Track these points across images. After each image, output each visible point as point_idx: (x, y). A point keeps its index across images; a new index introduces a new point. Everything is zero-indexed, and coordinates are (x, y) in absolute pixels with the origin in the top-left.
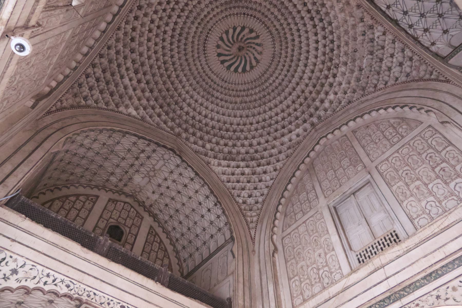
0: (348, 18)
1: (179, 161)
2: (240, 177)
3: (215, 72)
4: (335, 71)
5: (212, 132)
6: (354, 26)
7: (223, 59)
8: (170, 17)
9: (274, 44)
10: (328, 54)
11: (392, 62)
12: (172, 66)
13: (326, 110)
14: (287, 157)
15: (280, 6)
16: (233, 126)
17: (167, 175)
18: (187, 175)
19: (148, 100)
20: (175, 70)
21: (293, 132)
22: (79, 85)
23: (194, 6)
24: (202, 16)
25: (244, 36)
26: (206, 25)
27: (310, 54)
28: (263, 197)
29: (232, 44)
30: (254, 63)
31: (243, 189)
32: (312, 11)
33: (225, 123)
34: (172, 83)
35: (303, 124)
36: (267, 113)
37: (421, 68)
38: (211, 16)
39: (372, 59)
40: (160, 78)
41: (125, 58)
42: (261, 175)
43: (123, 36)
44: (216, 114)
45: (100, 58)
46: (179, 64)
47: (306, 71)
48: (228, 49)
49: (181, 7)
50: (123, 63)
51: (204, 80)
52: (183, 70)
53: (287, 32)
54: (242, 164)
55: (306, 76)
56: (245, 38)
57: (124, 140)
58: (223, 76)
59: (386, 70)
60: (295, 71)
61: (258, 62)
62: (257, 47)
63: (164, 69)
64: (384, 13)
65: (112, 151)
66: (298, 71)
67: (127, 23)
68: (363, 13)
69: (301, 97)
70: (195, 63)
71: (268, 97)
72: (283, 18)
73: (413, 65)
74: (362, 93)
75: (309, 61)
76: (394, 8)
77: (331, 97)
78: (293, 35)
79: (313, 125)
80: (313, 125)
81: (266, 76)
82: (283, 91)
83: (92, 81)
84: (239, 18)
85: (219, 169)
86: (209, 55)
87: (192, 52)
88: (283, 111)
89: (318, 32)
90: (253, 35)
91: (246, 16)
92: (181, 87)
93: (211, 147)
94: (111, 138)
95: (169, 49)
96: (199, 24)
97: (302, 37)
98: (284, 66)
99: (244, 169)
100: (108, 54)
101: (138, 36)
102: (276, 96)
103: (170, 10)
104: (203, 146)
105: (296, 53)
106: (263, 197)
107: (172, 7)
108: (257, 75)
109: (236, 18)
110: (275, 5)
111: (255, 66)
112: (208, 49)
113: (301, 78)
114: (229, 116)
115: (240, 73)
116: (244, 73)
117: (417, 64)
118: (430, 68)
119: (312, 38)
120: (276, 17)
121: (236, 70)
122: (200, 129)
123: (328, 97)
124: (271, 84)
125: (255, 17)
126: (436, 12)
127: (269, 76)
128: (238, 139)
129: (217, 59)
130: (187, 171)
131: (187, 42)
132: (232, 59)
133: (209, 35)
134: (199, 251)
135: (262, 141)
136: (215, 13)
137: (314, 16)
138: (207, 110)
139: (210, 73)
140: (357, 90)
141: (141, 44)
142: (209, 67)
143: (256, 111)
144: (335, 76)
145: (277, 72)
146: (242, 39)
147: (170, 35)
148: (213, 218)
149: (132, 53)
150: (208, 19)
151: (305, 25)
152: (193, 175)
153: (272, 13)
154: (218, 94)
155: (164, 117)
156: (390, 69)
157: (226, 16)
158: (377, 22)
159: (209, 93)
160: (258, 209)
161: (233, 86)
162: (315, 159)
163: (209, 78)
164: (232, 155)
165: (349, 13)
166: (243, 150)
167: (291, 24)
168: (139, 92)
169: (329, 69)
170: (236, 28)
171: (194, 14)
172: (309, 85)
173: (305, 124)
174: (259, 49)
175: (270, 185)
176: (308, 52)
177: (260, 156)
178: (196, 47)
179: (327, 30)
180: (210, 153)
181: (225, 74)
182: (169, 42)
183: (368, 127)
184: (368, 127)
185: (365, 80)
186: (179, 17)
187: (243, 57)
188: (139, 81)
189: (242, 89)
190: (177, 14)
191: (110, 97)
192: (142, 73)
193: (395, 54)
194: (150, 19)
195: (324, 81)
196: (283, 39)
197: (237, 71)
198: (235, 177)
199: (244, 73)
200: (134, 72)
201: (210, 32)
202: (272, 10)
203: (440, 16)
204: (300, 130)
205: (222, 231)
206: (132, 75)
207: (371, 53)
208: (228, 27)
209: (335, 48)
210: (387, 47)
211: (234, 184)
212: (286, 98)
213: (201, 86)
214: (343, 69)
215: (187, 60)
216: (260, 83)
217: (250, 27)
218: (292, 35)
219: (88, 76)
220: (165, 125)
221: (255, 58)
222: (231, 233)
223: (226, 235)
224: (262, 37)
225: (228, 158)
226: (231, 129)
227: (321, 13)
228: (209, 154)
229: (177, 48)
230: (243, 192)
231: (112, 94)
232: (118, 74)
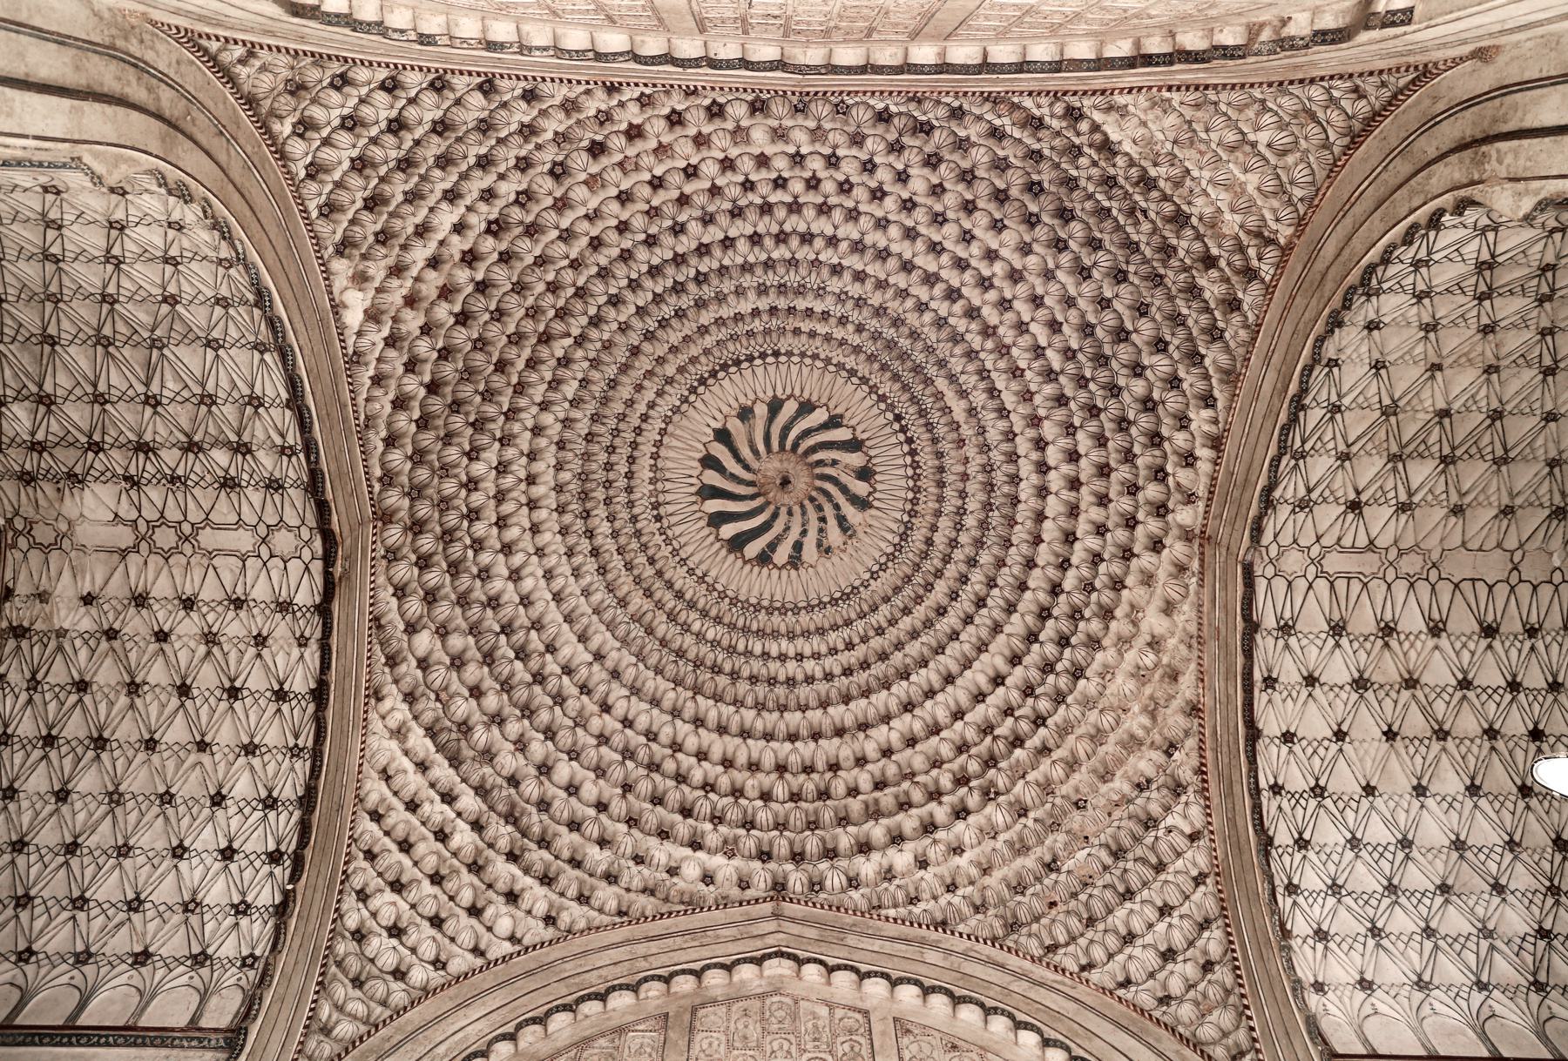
0: (1136, 708)
1: (306, 596)
2: (424, 839)
3: (660, 464)
4: (973, 801)
5: (476, 610)
6: (1133, 743)
8: (737, 213)
9: (883, 568)
10: (995, 738)
11: (1151, 926)
12: (584, 320)
13: (853, 882)
14: (620, 913)
16: (548, 657)
17: (210, 592)
18: (280, 660)
19: (426, 330)
20: (580, 341)
21: (700, 854)
22: (342, 76)
23: (816, 263)
24: (801, 304)
25: (835, 463)
26: (782, 331)
27: (950, 689)
28: (437, 977)
30: (782, 554)
31: (397, 886)
32: (1062, 598)
33: (537, 625)
34: (532, 363)
35: (751, 857)
36: (679, 723)
37: (1216, 1013)
38: (822, 329)
39: (1105, 868)
41: (524, 164)
42: (491, 894)
43: (592, 112)
44: (540, 573)
45: (480, 87)
46: (606, 336)
47: (895, 723)
48: (761, 448)
49: (787, 228)
50: (502, 169)
51: (611, 449)
52: (595, 363)
53: (947, 574)
54: (469, 801)
55: (880, 734)
56: (828, 471)
57: (240, 360)
58: (669, 497)
59: (1116, 932)
60: (866, 693)
61: (795, 561)
62: (832, 522)
63: (561, 303)
64: (1256, 792)
65: (156, 344)
66: (873, 698)
67: (644, 101)
68: (1187, 733)
69: (815, 776)
70: (646, 383)
71: (723, 681)
72: (976, 533)
73: (1201, 987)
74: (1000, 932)
75: (929, 704)
76: (1285, 805)
77: (901, 859)
79: (779, 887)
80: (779, 887)
81: (776, 619)
82: (783, 708)
83: (381, 109)
84: (875, 411)
85: (385, 748)
86: (699, 404)
87: (674, 350)
88: (728, 763)
89: (1027, 660)
90: (860, 488)
91: (896, 426)
92: (538, 399)
93: (431, 652)
94: (219, 311)
95: (634, 276)
97: (971, 629)
98: (850, 646)
99: (460, 824)
100: (504, 105)
101: (618, 157)
102: (749, 701)
103: (759, 201)
104: (411, 628)
105: (914, 649)
106: (433, 974)
107: (772, 199)
108: (755, 592)
113: (864, 726)
114: (568, 619)
115: (718, 539)
117: (1214, 993)
118: (1242, 1036)
119: (994, 659)
120: (961, 512)
121: (717, 520)
122: (455, 568)
123: (892, 852)
124: (765, 655)
125: (913, 453)
126: (1371, 912)
127: (783, 629)
128: (528, 711)
129: (705, 439)
130: (296, 652)
132: (740, 481)
133: (758, 362)
134: (30, 969)
135: (590, 790)
136: (839, 333)
137: (1056, 612)
138: (528, 534)
139: (647, 449)
140: (991, 912)
141: (593, 182)
142: (663, 432)
143: (652, 683)
144: (961, 813)
145: (816, 644)
146: (820, 463)
147: (680, 250)
148: (217, 893)
149: (551, 172)
150: (806, 326)
151: (1011, 608)
152: (301, 683)
153: (963, 494)
154: (605, 528)
155: (404, 422)
156: (1129, 938)
157: (852, 373)
158: (1203, 791)
159: (584, 496)
160: (384, 1003)
161: (666, 551)
162: (714, 1002)
163: (632, 460)
164: (463, 743)
165: (1152, 698)
166: (509, 761)
168: (434, 279)
169: (962, 780)
170: (838, 425)
171: (792, 278)
172: (869, 767)
173: (757, 864)
174: (834, 535)
175: (491, 956)
176: (949, 679)
177: (544, 831)
178: (694, 350)
179: (1051, 679)
180: (409, 668)
181: (680, 496)
182: (656, 261)
183: (954, 1047)
184: (954, 1047)
185: (1038, 907)
188: (470, 258)
189: (677, 586)
190: (761, 229)
191: (359, 204)
192: (503, 246)
193: (1176, 913)
195: (917, 795)
196: (918, 579)
197: (717, 527)
198: (407, 822)
200: (490, 223)
201: (770, 359)
202: (972, 487)
203: (1375, 932)
204: (725, 868)
205: (205, 972)
206: (477, 222)
207: (1118, 853)
209: (1028, 744)
210: (1170, 878)
211: (386, 840)
212: (768, 736)
213: (587, 457)
214: (997, 814)
215: (635, 351)
216: (740, 623)
218: (954, 596)
219: (391, 86)
220: (380, 446)
221: (798, 546)
222: (248, 1012)
223: (214, 1002)
225: (443, 737)
226: (534, 664)
227: (1082, 625)
228: (403, 668)
229: (650, 297)
230: (389, 896)
231: (373, 203)
232: (455, 178)
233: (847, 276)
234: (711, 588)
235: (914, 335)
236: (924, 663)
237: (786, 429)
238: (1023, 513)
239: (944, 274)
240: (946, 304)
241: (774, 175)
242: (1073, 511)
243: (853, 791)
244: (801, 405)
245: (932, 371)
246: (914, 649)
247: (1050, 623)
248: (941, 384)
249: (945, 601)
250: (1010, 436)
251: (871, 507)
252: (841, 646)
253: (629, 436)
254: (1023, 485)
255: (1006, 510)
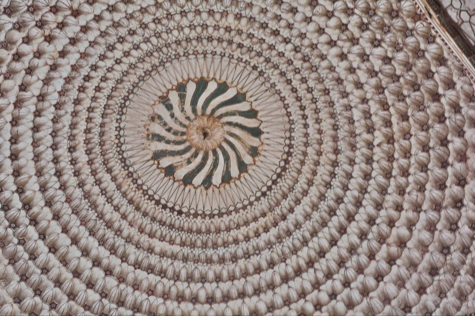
3: (277, 96)
7: (249, 120)
9: (118, 137)
12: (375, 158)
15: (97, 227)
23: (284, 260)
24: (274, 231)
25: (189, 162)
26: (271, 209)
27: (31, 125)
29: (221, 147)
30: (174, 98)
32: (27, 221)
40: (413, 152)
48: (231, 139)
49: (311, 271)
51: (310, 90)
56: (188, 155)
58: (258, 82)
61: (164, 100)
62: (163, 133)
78: (71, 161)
81: (147, 66)
84: (193, 206)
86: (282, 141)
87: (317, 163)
89: (11, 179)
90: (166, 162)
91: (177, 208)
95: (367, 196)
96: (284, 218)
98: (98, 89)
103: (335, 276)
105: (67, 120)
108: (171, 69)
109: (200, 207)
110: (109, 227)
111: (172, 89)
112: (279, 155)
115: (214, 79)
116: (202, 78)
120: (110, 200)
124: (137, 47)
125: (158, 203)
127: (140, 65)
131: (323, 189)
132: (227, 114)
133: (270, 183)
136: (244, 230)
139: (290, 100)
141: (423, 247)
145: (116, 75)
146: (195, 155)
147: (353, 224)
151: (43, 188)
153: (117, 208)
157: (220, 215)
163: (294, 90)
167: (75, 184)
170: (204, 183)
171: (288, 242)
174: (157, 128)
176: (36, 129)
181: (253, 87)
186: (322, 253)
187: (199, 113)
189: (215, 43)
194: (381, 284)
197: (219, 84)
199: (202, 78)
200: (463, 205)
201: (264, 189)
202: (116, 216)
208: (222, 189)
213: (320, 80)
215: (336, 151)
216: (165, 50)
217: (172, 181)
218: (73, 162)
221: (169, 107)
224: (148, 154)
229: (350, 186)
233: (264, 264)
234: (196, 53)
235: (209, 261)
236: (55, 120)
237: (227, 159)
238: (83, 232)
239: (223, 305)
240: (209, 291)
241: (339, 297)
242: (64, 261)
243: (27, 40)
244: (231, 178)
245: (186, 250)
246: (67, 120)
247: (20, 205)
248: (176, 248)
249: (75, 154)
250: (124, 258)
251: (152, 158)
252: (103, 85)
253: (305, 102)
254: (96, 244)
255: (91, 224)
